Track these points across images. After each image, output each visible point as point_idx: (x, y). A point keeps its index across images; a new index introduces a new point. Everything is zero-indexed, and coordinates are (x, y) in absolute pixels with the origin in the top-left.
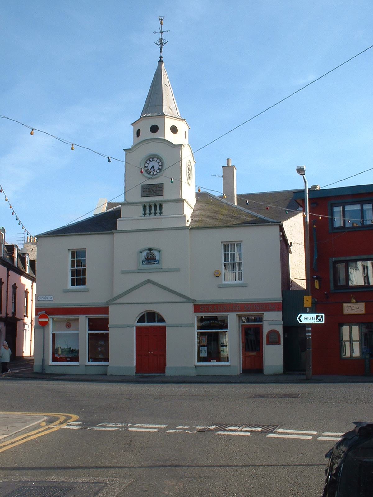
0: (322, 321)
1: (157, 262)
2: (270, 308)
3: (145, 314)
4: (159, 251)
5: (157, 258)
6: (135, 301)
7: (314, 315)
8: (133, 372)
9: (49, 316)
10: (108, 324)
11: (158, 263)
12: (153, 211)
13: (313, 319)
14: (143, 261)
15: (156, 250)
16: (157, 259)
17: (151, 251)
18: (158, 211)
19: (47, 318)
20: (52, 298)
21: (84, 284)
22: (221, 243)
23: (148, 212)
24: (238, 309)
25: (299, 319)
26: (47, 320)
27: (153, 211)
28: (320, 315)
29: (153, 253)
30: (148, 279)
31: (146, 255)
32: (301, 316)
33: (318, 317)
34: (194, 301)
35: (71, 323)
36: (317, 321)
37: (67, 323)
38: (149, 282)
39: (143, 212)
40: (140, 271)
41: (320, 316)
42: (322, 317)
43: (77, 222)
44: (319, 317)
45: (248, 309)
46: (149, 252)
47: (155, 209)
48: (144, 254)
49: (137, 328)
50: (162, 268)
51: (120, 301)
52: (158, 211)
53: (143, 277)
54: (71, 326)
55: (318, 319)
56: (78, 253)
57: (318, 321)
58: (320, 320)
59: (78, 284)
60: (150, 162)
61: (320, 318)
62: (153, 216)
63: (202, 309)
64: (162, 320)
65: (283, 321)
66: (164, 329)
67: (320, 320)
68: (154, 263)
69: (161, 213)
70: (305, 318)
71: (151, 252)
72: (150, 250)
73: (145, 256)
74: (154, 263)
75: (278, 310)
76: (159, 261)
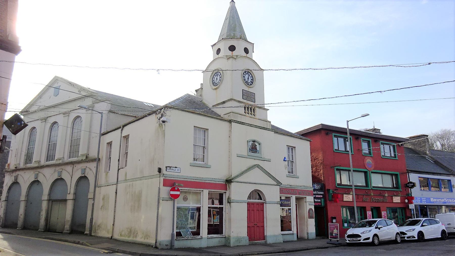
1: (258, 152)
4: (259, 144)
6: (249, 181)
14: (250, 150)
15: (257, 142)
19: (178, 190)
26: (178, 193)
35: (187, 196)
37: (184, 196)
46: (253, 143)
52: (253, 113)
54: (187, 199)
60: (245, 75)
66: (262, 204)
72: (254, 141)
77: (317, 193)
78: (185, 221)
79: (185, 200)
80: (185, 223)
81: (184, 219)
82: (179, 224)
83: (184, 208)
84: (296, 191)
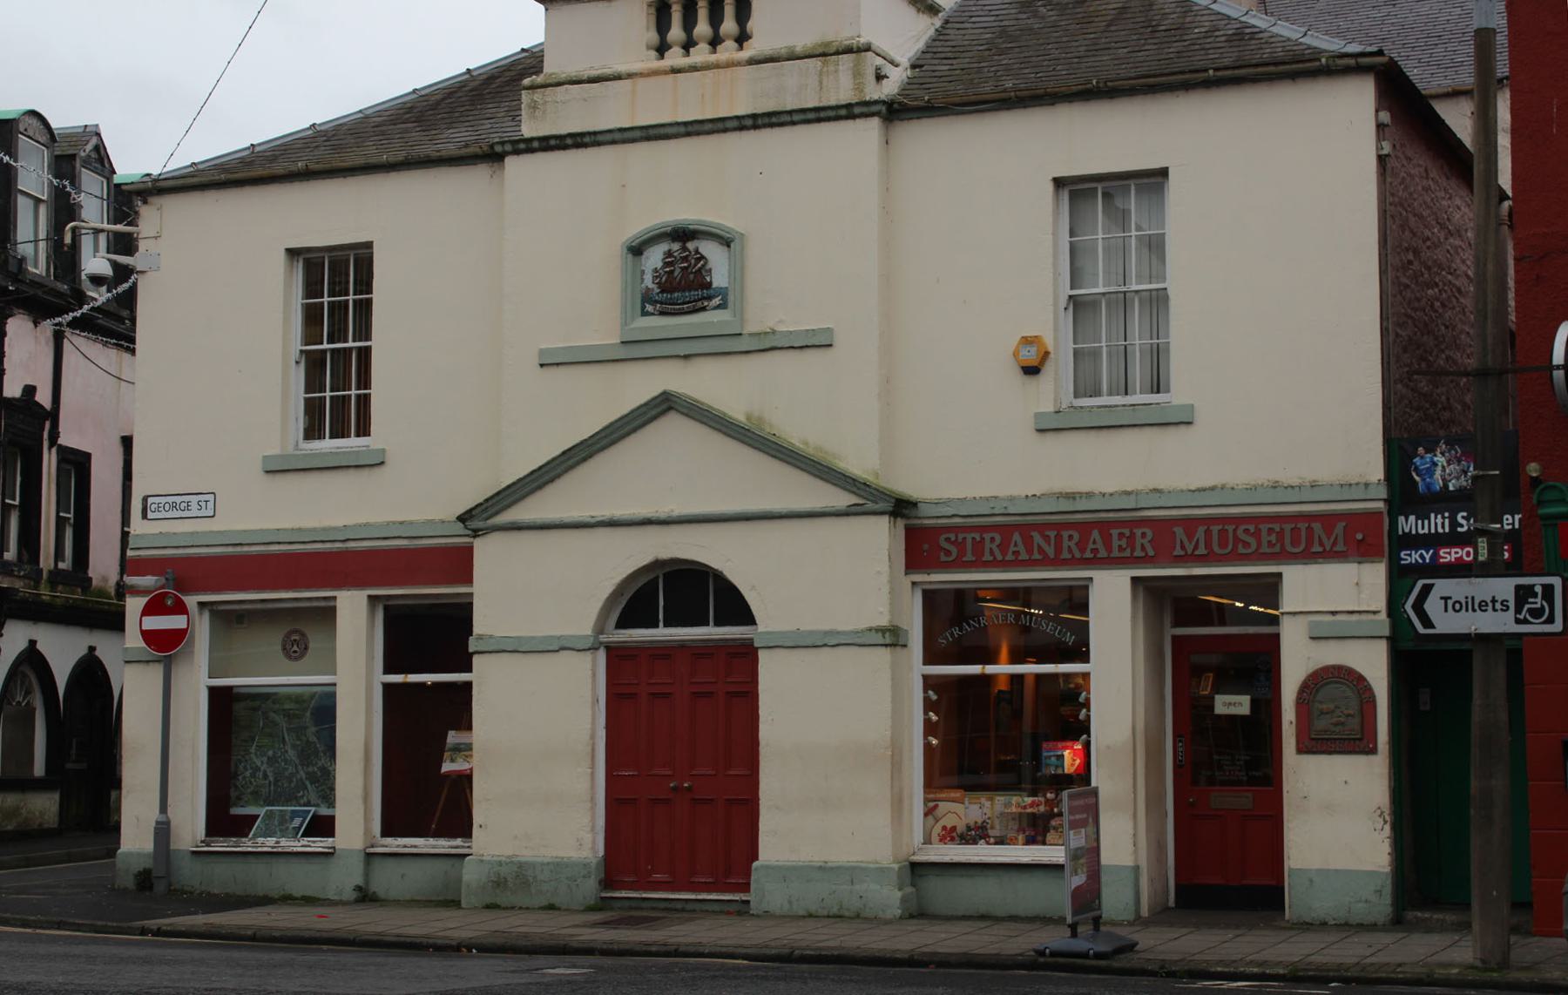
0: (1551, 620)
1: (716, 301)
2: (1317, 548)
3: (657, 578)
4: (727, 242)
5: (719, 279)
7: (1504, 588)
8: (589, 888)
9: (191, 601)
10: (470, 632)
11: (723, 306)
12: (702, 28)
13: (1498, 606)
14: (647, 298)
16: (715, 285)
17: (691, 245)
18: (729, 26)
19: (180, 608)
20: (211, 505)
21: (364, 429)
22: (1050, 187)
23: (676, 33)
24: (1143, 548)
25: (1419, 607)
27: (702, 28)
28: (1537, 582)
29: (697, 251)
30: (664, 393)
31: (659, 265)
32: (1427, 590)
33: (1523, 594)
34: (901, 507)
36: (1518, 621)
38: (670, 408)
39: (653, 36)
40: (633, 351)
41: (1538, 589)
42: (1548, 591)
43: (360, 111)
44: (1535, 595)
45: (1196, 547)
46: (676, 246)
47: (716, 19)
48: (654, 258)
49: (618, 658)
50: (744, 332)
51: (527, 511)
52: (729, 26)
53: (641, 384)
54: (306, 648)
55: (1527, 606)
56: (339, 268)
57: (1525, 621)
58: (1536, 613)
59: (340, 432)
61: (1538, 602)
62: (700, 54)
63: (948, 553)
64: (735, 608)
65: (1389, 615)
66: (746, 655)
67: (1536, 613)
68: (699, 304)
69: (742, 38)
70: (1450, 603)
71: (684, 249)
72: (682, 234)
73: (656, 270)
74: (699, 304)
75: (1362, 551)
76: (723, 292)
77: (1454, 524)
78: (297, 762)
79: (295, 652)
80: (297, 772)
81: (292, 754)
82: (265, 776)
83: (289, 698)
84: (1138, 532)
